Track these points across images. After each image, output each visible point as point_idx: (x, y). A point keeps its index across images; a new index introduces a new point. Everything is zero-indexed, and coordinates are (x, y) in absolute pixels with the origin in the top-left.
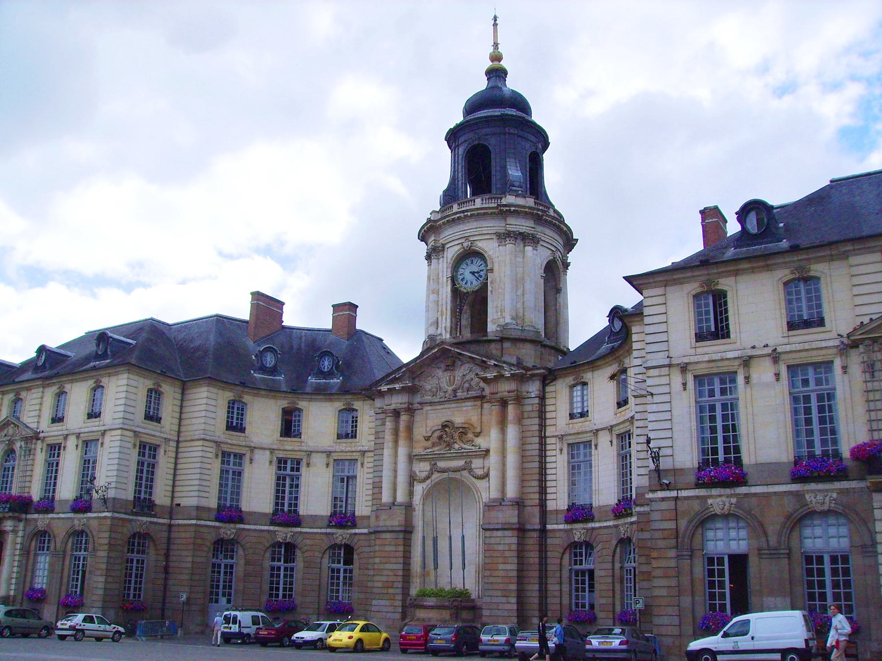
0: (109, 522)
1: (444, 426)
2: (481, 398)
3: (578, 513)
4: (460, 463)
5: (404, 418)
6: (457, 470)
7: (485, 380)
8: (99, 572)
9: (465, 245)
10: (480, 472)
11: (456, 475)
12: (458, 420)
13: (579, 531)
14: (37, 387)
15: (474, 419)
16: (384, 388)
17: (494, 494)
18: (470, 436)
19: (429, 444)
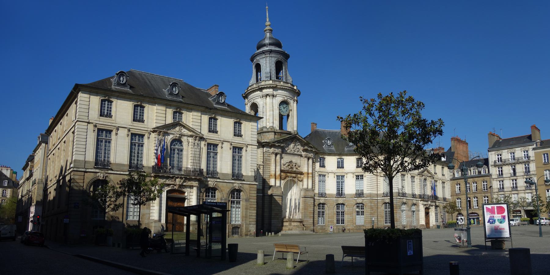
0: (255, 186)
1: (290, 162)
2: (301, 156)
3: (322, 195)
4: (294, 175)
5: (278, 156)
6: (294, 177)
7: (304, 150)
8: (253, 209)
9: (286, 98)
10: (300, 179)
11: (294, 179)
12: (294, 161)
13: (322, 200)
14: (197, 111)
15: (298, 162)
16: (277, 145)
17: (305, 186)
18: (297, 167)
19: (285, 167)
